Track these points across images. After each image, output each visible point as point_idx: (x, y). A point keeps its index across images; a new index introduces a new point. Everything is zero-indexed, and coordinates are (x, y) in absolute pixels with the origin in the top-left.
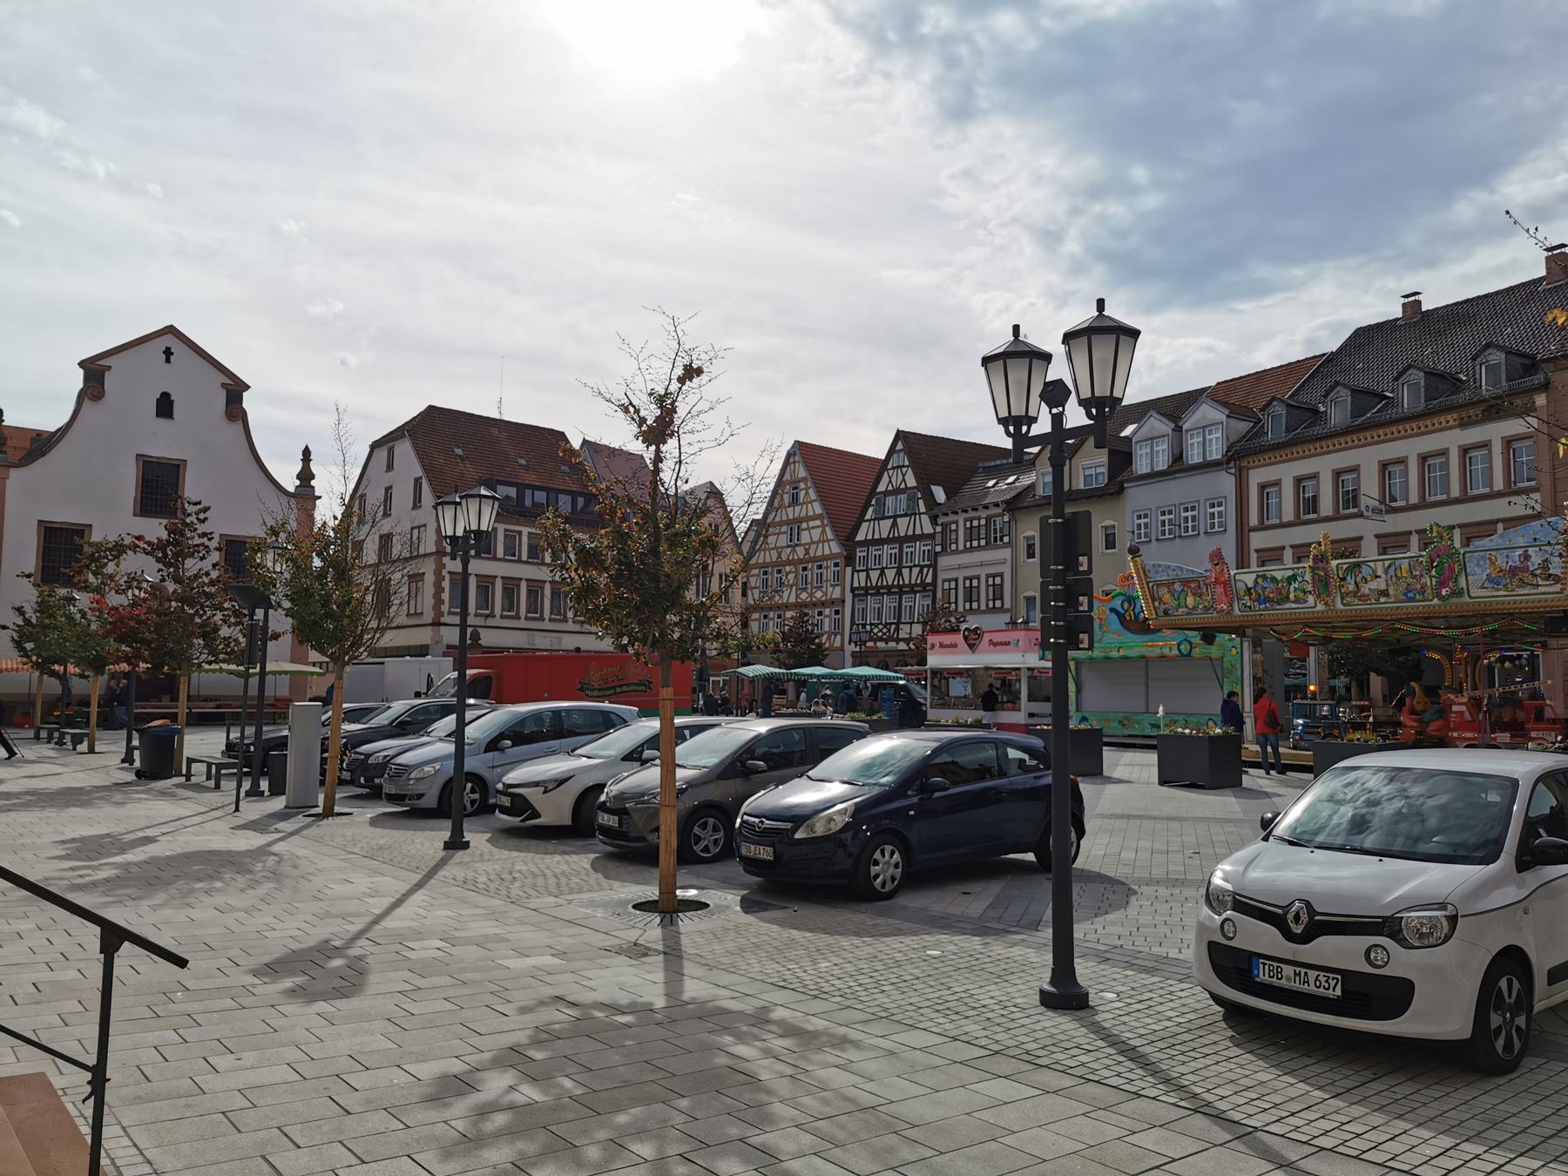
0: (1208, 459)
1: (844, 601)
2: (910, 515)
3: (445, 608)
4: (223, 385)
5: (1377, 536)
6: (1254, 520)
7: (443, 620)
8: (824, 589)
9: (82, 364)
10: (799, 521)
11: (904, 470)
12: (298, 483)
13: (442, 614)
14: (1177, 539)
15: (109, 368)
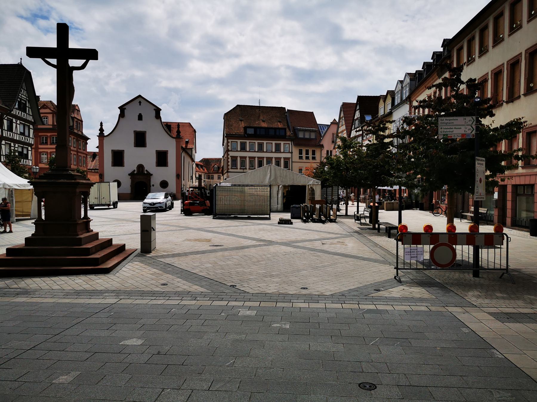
3: (230, 167)
4: (154, 109)
7: (229, 171)
9: (119, 108)
12: (100, 132)
13: (229, 169)
15: (125, 109)
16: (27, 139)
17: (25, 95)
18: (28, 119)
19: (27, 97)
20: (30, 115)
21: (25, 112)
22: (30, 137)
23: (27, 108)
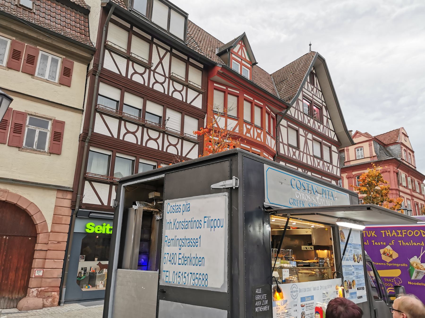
16: (328, 167)
17: (318, 96)
18: (327, 135)
19: (322, 101)
20: (331, 130)
21: (322, 123)
22: (334, 164)
23: (325, 119)
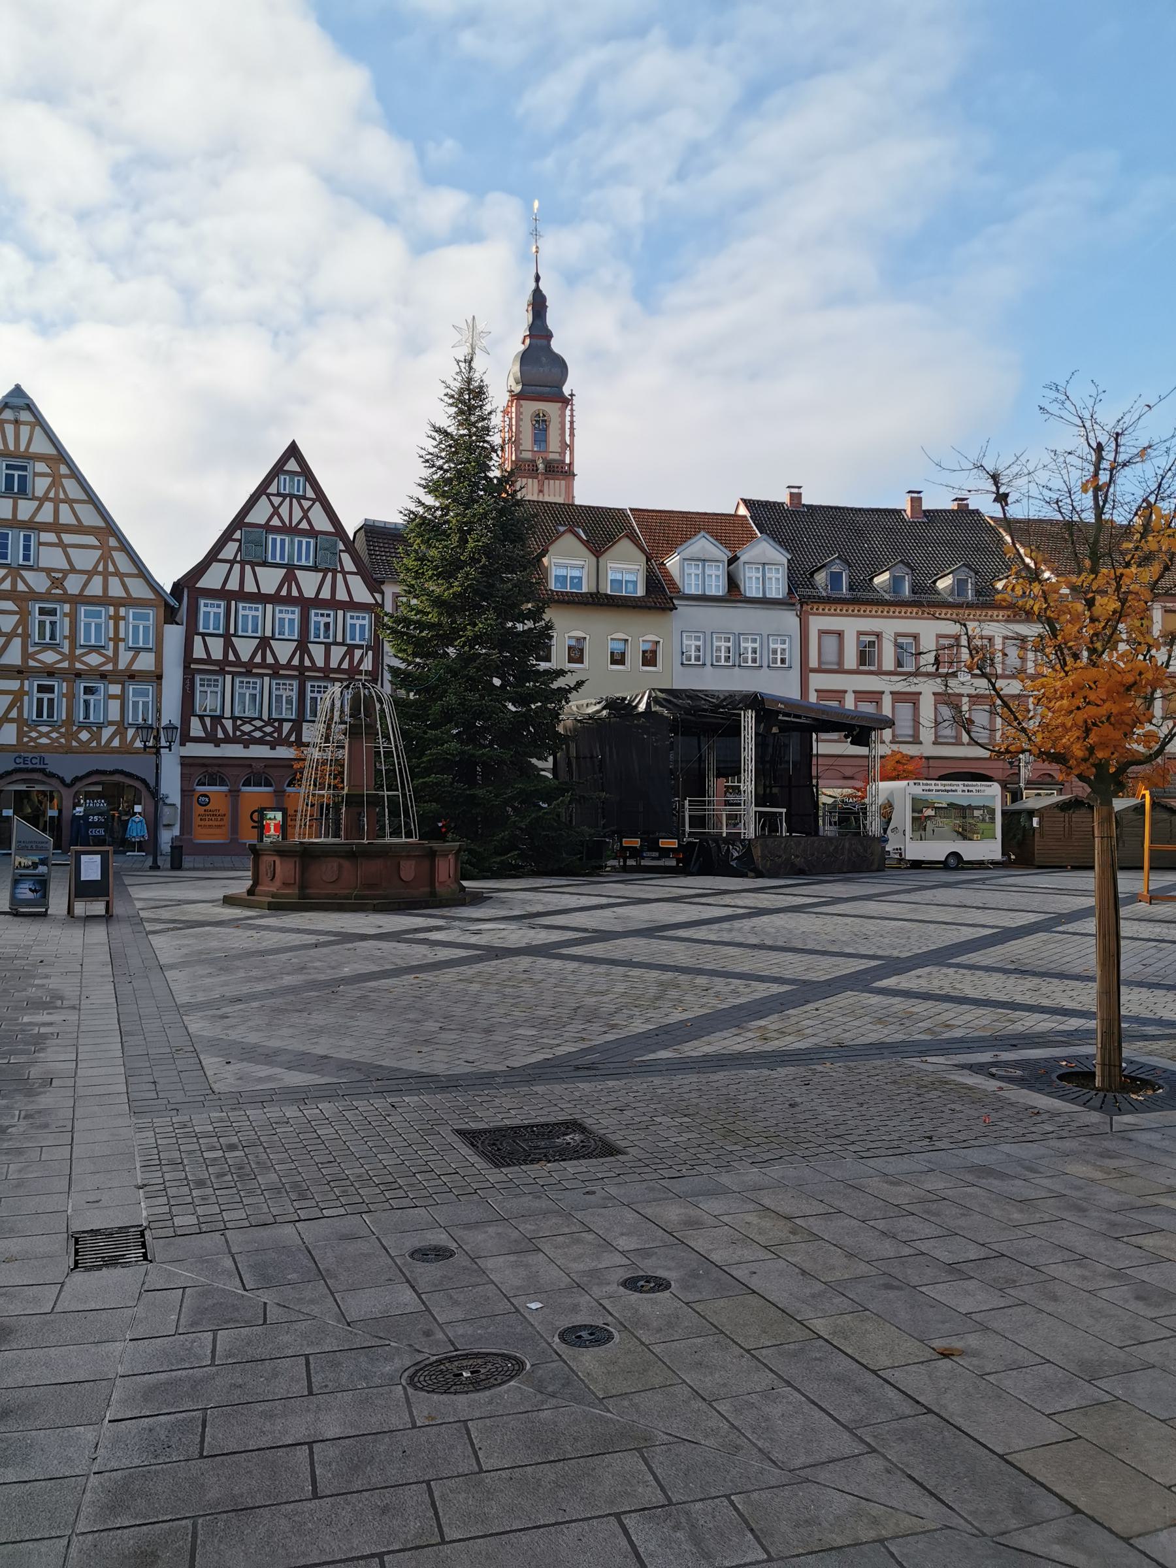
0: (768, 596)
1: (160, 677)
2: (325, 571)
5: (934, 694)
6: (813, 663)
8: (110, 653)
10: (32, 526)
11: (306, 504)
14: (737, 668)
